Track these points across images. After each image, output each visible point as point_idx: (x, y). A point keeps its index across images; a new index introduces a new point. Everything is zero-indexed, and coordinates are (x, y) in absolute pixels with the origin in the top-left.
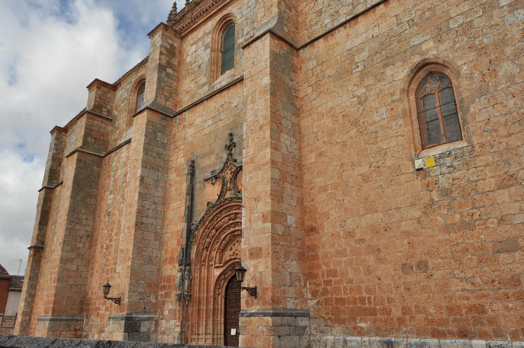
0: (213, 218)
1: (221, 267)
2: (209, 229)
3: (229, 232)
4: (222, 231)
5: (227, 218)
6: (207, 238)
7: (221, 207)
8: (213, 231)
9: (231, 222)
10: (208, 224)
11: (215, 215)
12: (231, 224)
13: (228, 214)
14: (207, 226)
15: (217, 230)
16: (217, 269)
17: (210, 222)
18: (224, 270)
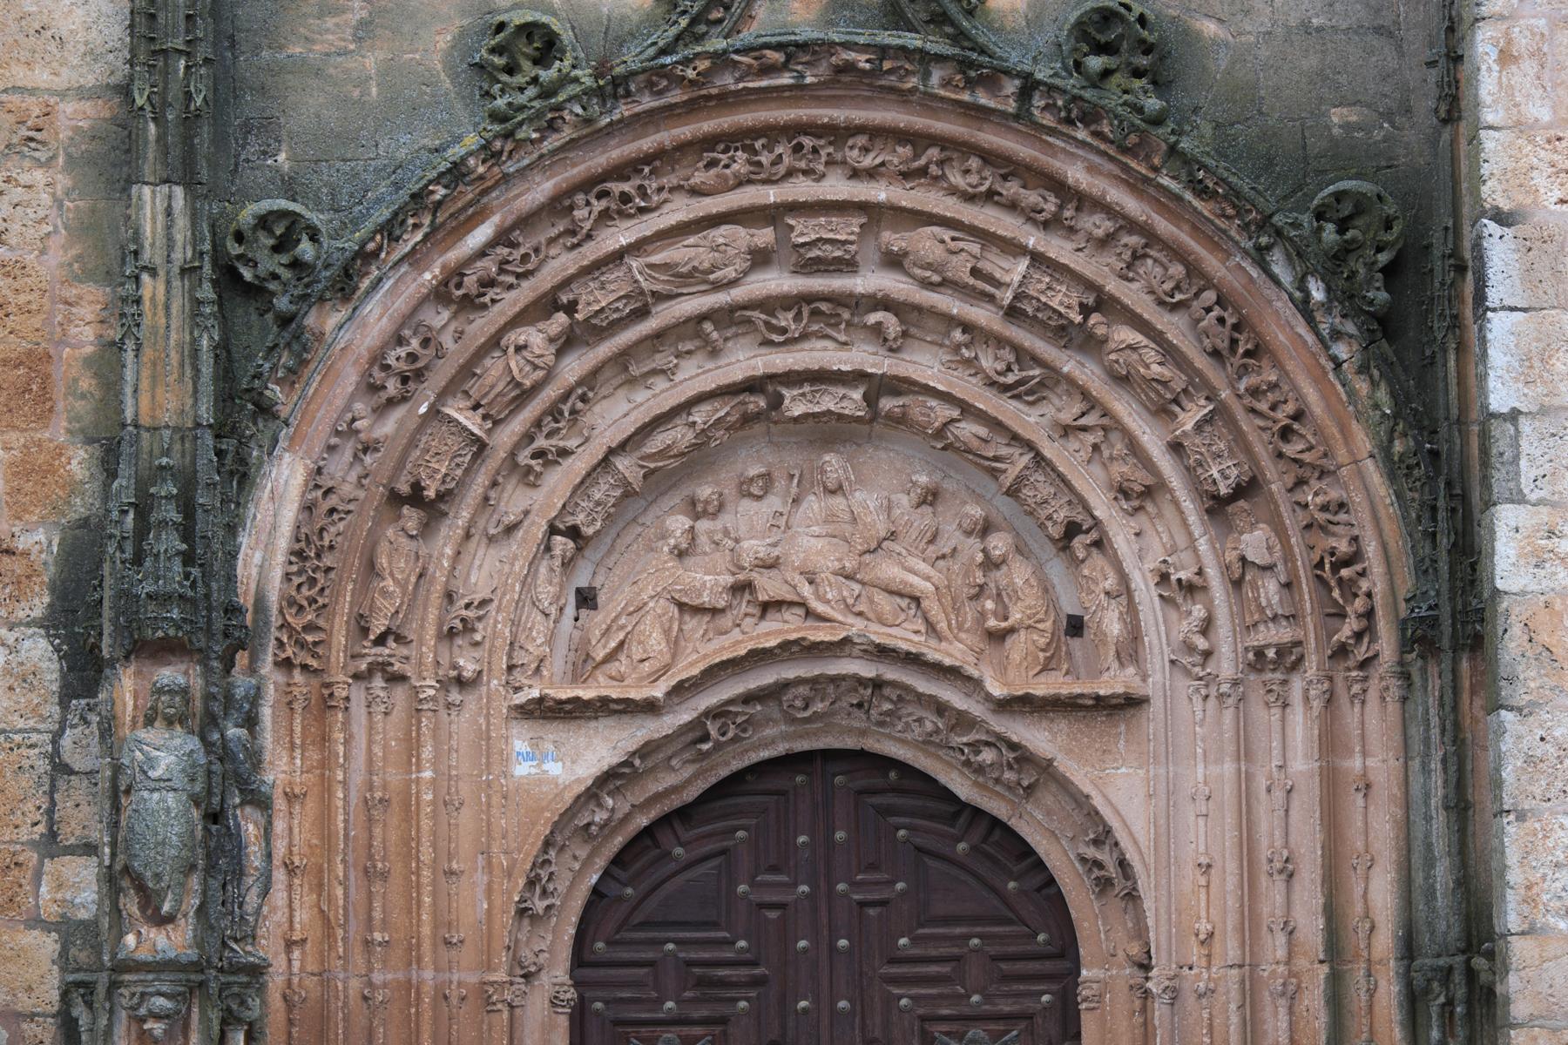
0: (558, 205)
1: (650, 707)
2: (470, 304)
3: (696, 375)
4: (622, 359)
5: (741, 237)
7: (692, 108)
8: (535, 337)
9: (776, 281)
10: (482, 253)
11: (588, 184)
12: (769, 305)
13: (772, 195)
14: (456, 274)
15: (566, 343)
16: (553, 733)
17: (503, 238)
18: (646, 750)
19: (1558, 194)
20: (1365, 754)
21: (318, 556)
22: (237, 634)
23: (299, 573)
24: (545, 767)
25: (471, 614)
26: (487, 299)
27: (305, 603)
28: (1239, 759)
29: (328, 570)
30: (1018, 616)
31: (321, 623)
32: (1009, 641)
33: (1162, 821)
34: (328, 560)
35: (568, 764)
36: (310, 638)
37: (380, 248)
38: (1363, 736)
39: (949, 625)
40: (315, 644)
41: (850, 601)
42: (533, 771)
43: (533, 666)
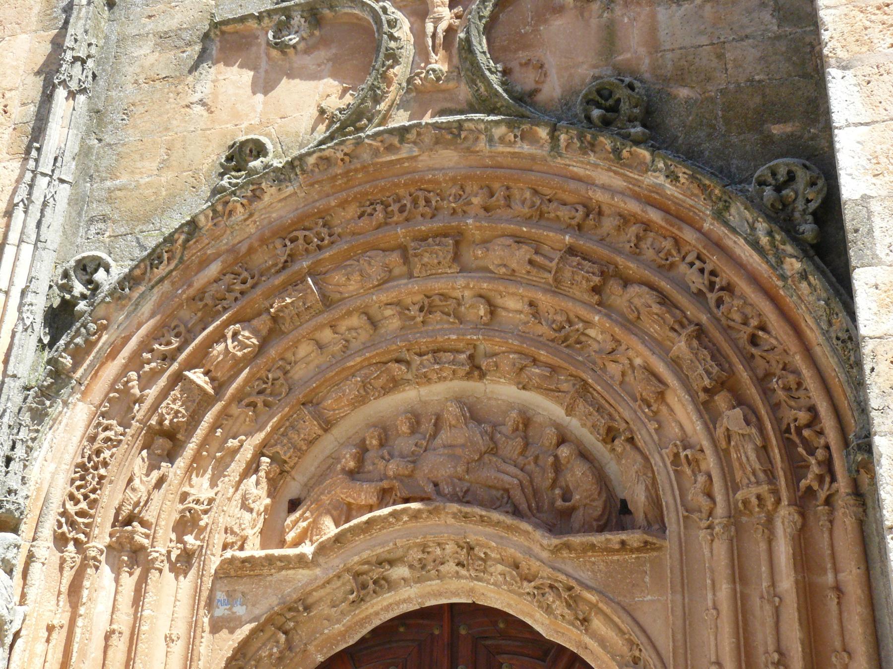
6: (191, 365)
19: (890, 41)
20: (836, 571)
21: (96, 468)
22: (8, 506)
23: (82, 478)
24: (235, 609)
25: (198, 507)
26: (219, 307)
27: (81, 498)
28: (734, 582)
29: (101, 477)
30: (578, 497)
31: (92, 512)
32: (574, 516)
33: (679, 636)
34: (102, 471)
35: (250, 607)
36: (80, 520)
37: (144, 273)
38: (833, 555)
39: (529, 507)
40: (87, 525)
41: (460, 494)
42: (227, 612)
43: (239, 543)
